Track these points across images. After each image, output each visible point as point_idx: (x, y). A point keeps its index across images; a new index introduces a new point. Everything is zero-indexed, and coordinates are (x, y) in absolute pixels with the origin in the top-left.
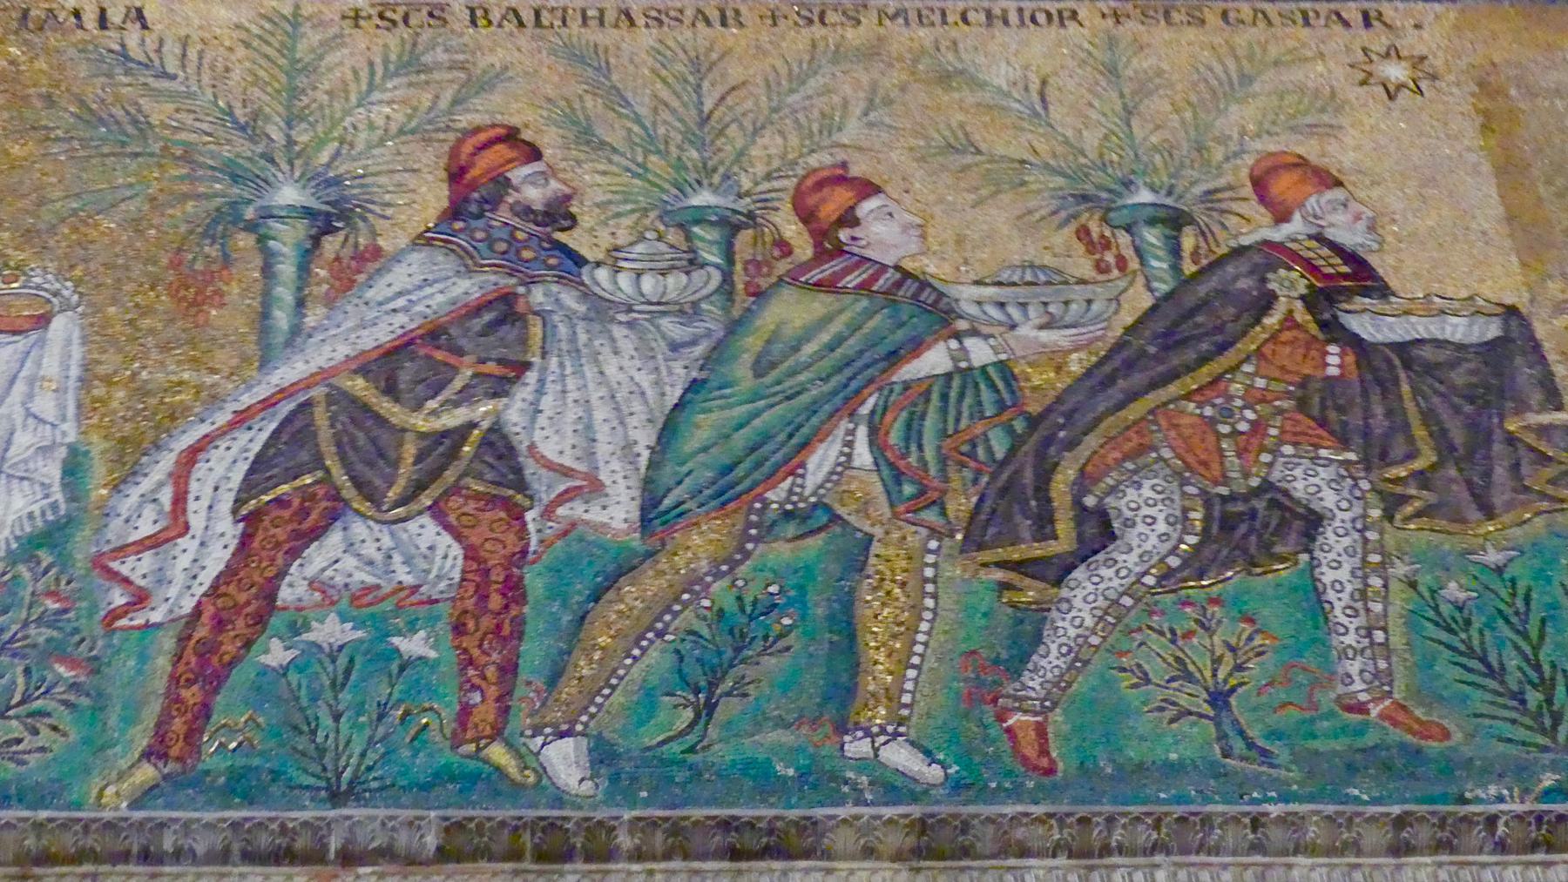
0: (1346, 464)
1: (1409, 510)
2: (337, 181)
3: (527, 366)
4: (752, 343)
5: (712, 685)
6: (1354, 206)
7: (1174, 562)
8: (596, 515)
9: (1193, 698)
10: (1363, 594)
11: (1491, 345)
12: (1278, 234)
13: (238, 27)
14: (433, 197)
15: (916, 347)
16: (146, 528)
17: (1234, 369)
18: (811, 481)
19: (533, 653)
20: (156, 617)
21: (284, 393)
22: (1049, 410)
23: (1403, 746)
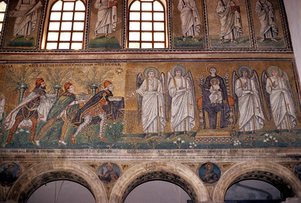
0: (105, 114)
1: (109, 119)
2: (27, 85)
3: (40, 104)
4: (58, 101)
5: (50, 135)
6: (112, 86)
7: (88, 124)
8: (43, 119)
9: (87, 137)
10: (103, 127)
11: (120, 101)
12: (104, 90)
13: (20, 67)
14: (34, 86)
15: (72, 102)
16: (8, 120)
17: (98, 104)
18: (61, 115)
19: (37, 132)
20: (8, 129)
21: (20, 107)
22: (81, 109)
23: (102, 142)
